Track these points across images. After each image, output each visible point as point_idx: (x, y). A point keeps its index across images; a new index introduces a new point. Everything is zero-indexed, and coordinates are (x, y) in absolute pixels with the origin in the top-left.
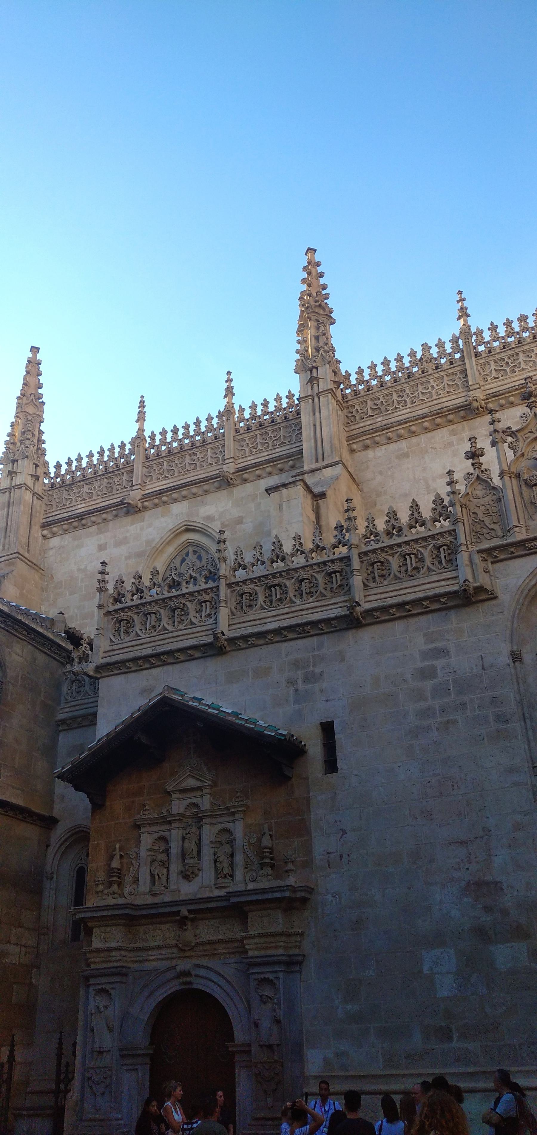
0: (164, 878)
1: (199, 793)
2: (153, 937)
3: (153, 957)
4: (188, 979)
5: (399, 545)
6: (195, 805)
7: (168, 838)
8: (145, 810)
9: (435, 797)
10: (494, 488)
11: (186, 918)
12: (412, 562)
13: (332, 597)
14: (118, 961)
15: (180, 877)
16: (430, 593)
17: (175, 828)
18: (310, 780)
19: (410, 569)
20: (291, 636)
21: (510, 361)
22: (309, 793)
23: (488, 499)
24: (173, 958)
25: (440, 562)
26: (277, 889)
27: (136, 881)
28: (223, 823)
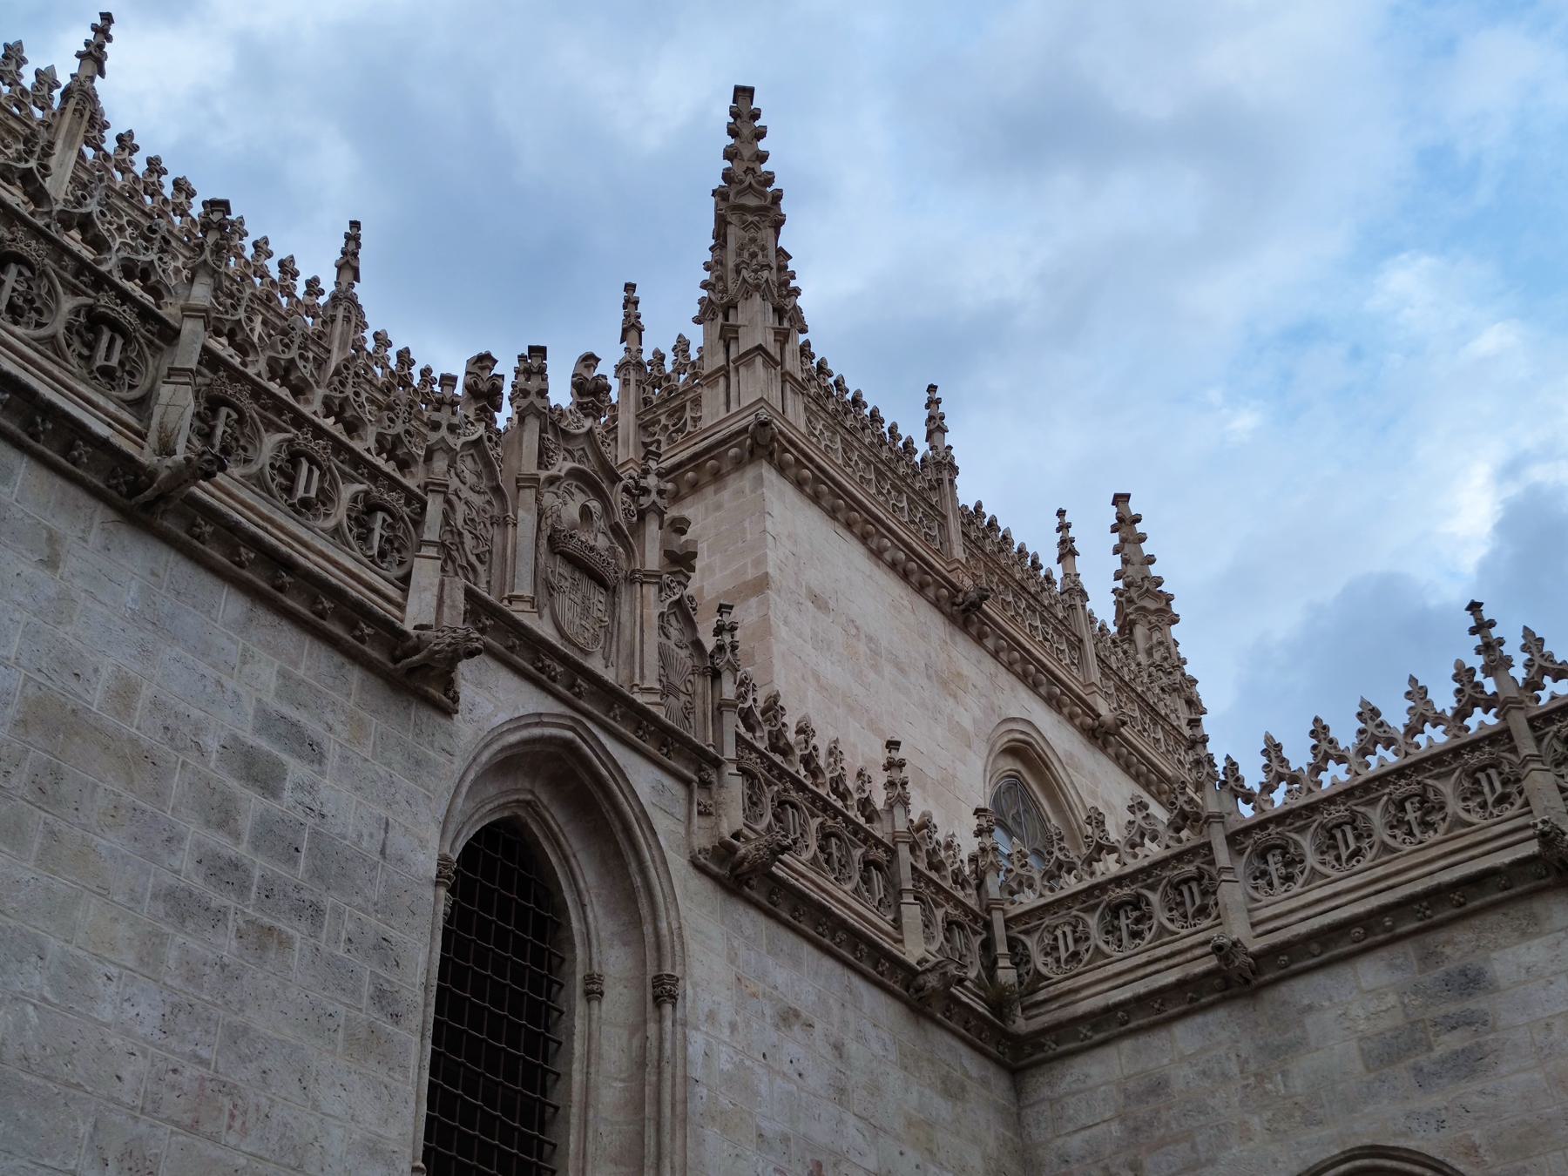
5: (299, 420)
9: (177, 1124)
10: (497, 490)
12: (307, 483)
13: (83, 381)
16: (355, 591)
19: (300, 493)
21: (129, 230)
23: (478, 500)
25: (364, 538)
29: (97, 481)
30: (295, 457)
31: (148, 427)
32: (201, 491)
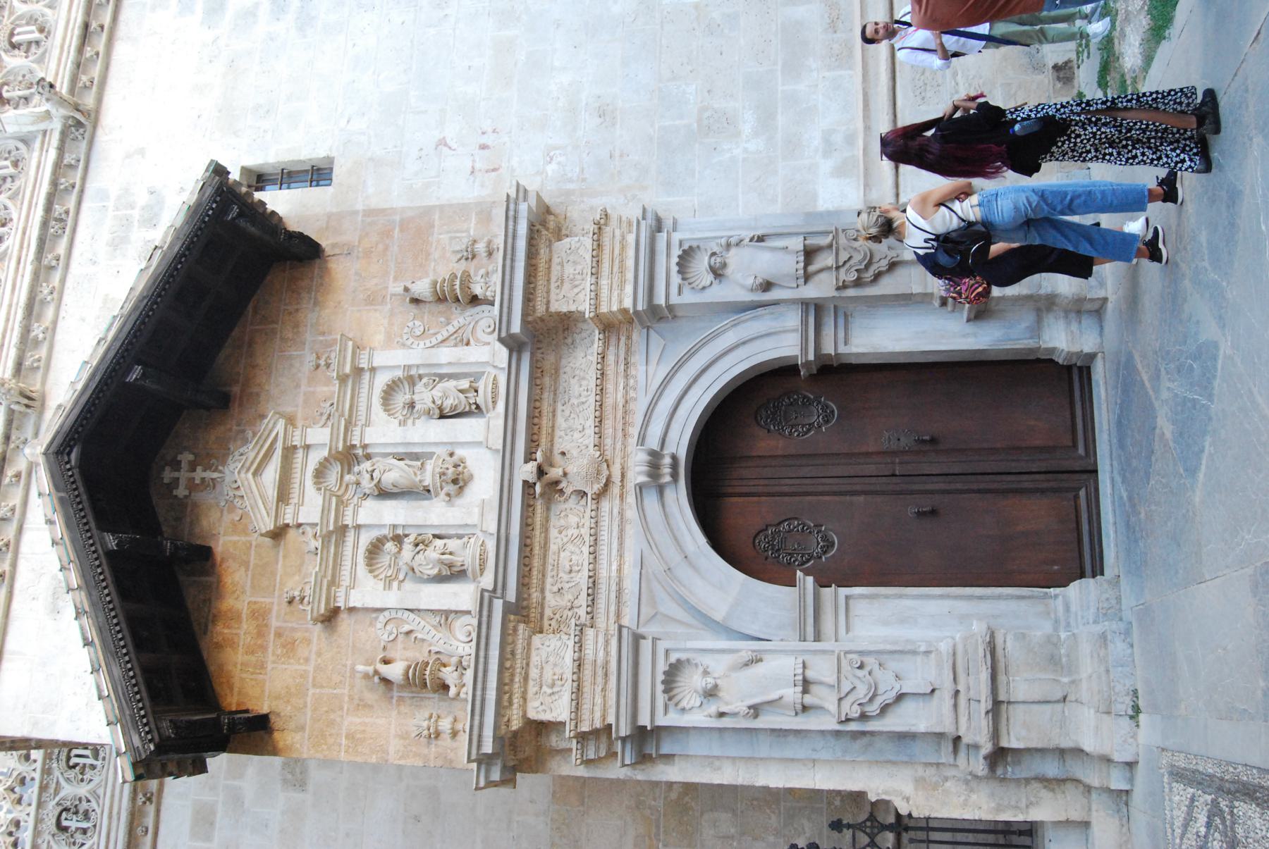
0: (453, 544)
1: (300, 454)
2: (571, 571)
3: (614, 567)
4: (667, 460)
6: (320, 474)
7: (375, 533)
8: (302, 599)
11: (541, 472)
12: (26, 34)
13: (27, 174)
14: (607, 642)
15: (459, 501)
17: (355, 513)
18: (334, 210)
20: (61, 249)
22: (356, 212)
24: (621, 513)
26: (511, 223)
27: (447, 616)
28: (369, 399)
29: (83, 145)
30: (14, 46)
31: (38, 131)
32: (63, 87)
